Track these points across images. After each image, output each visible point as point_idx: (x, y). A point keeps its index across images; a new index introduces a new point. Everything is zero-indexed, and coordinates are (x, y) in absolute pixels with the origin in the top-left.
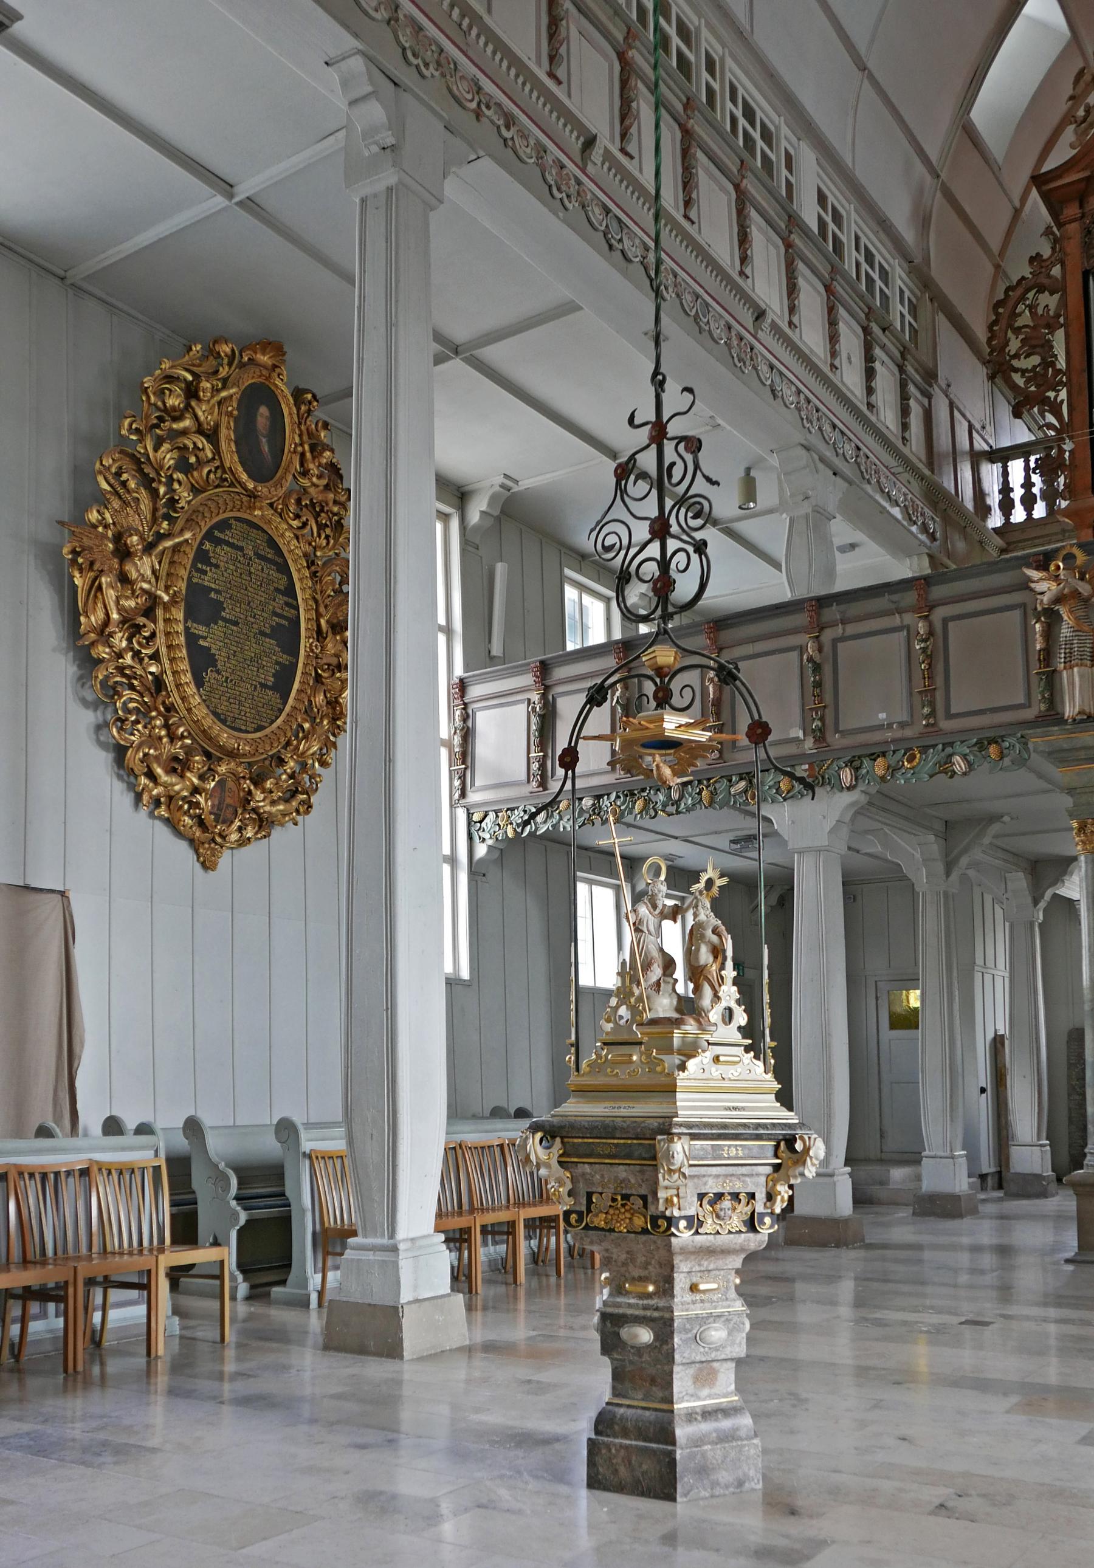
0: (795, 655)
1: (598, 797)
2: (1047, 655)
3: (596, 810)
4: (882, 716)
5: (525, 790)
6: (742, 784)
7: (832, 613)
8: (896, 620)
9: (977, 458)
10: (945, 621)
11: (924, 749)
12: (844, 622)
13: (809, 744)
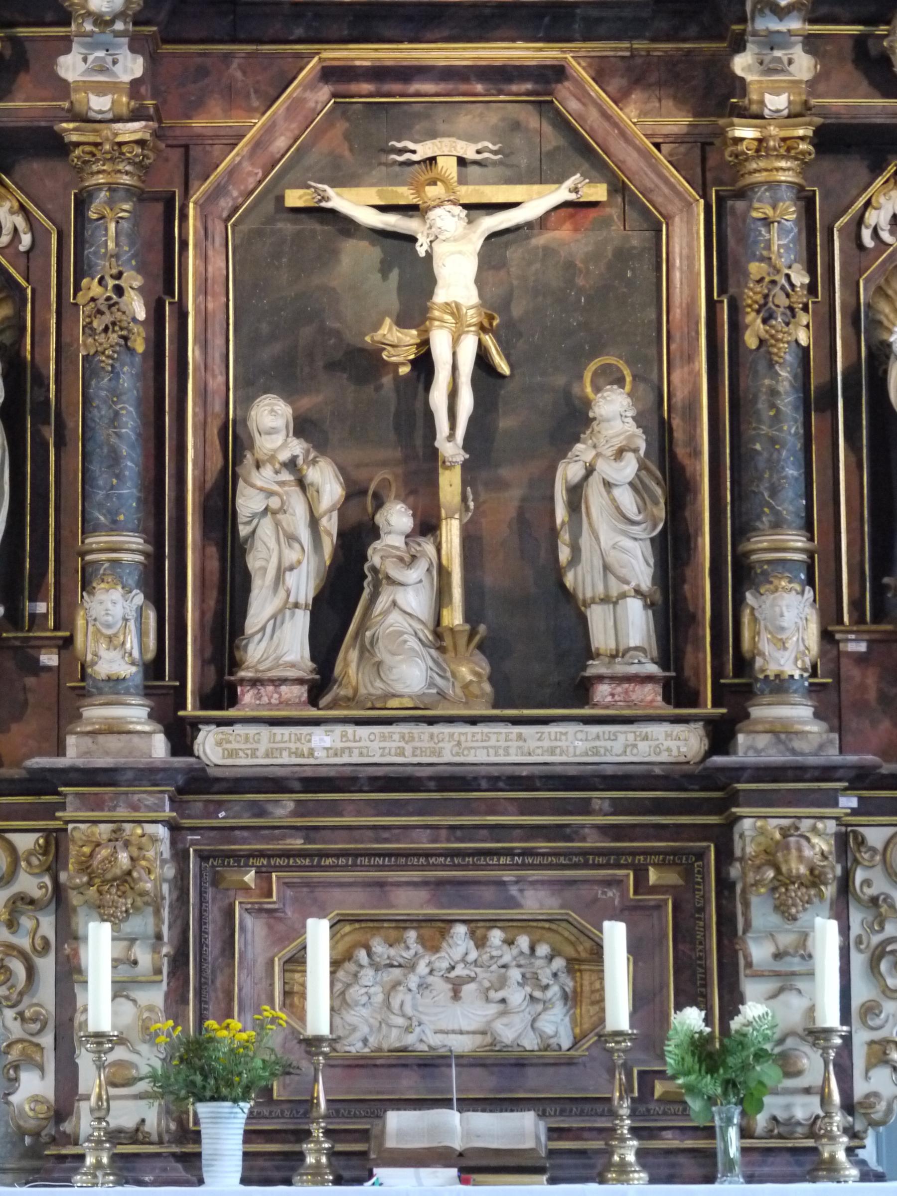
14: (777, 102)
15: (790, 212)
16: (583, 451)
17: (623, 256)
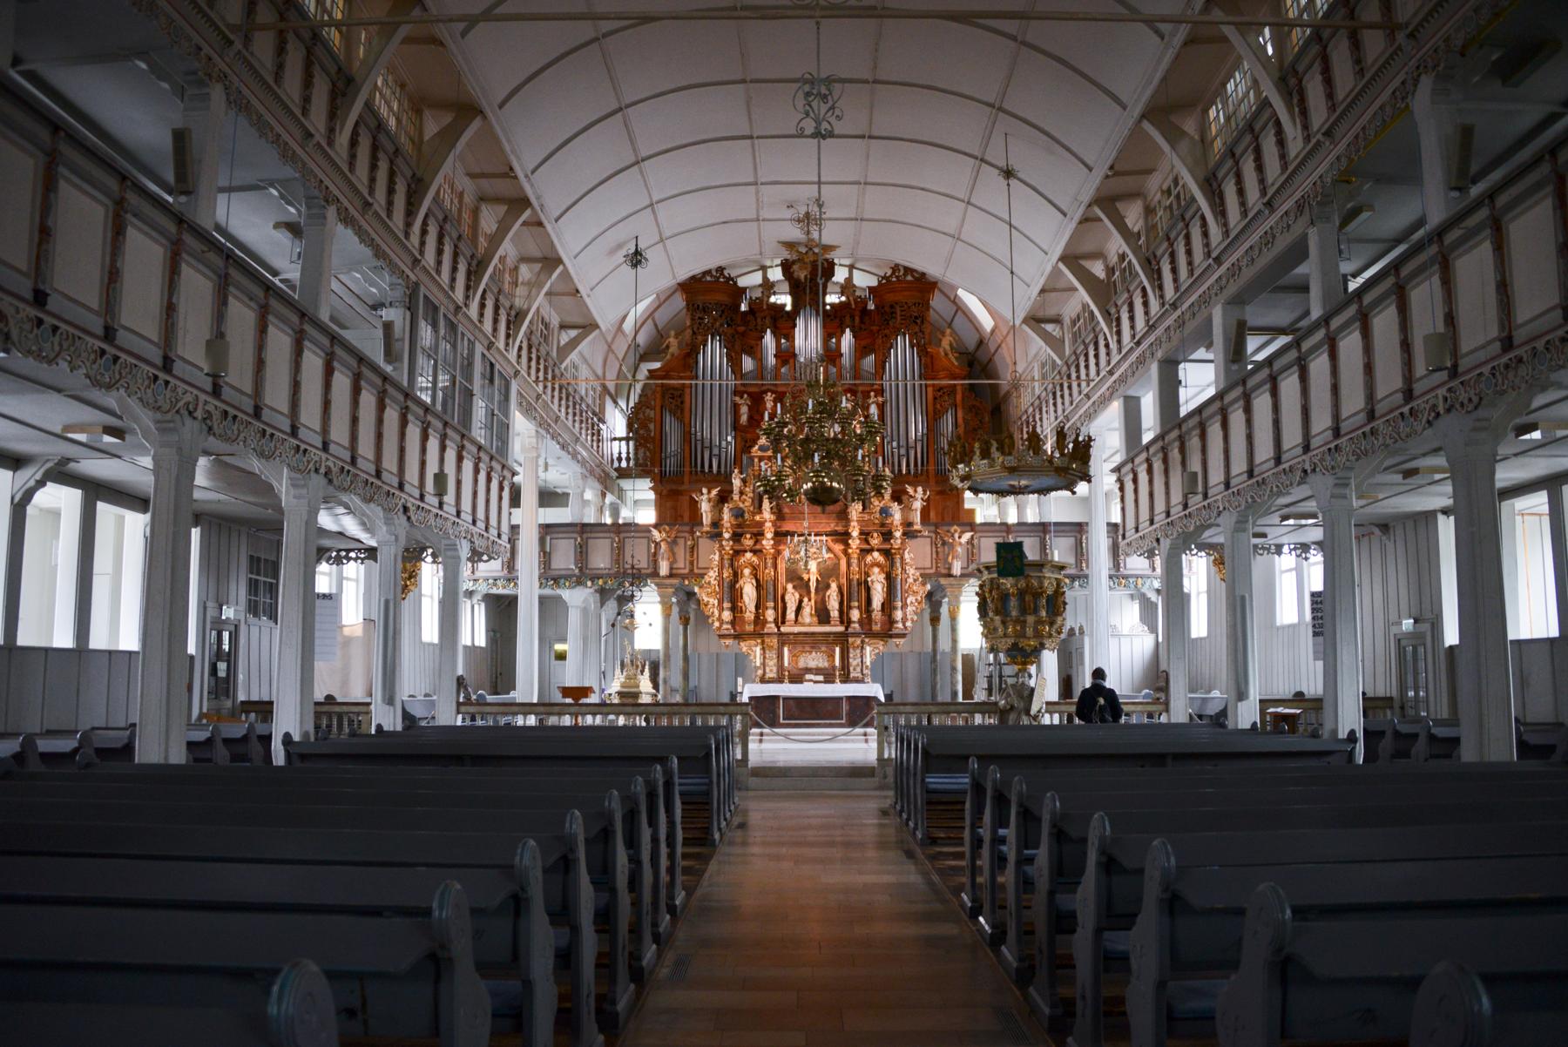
0: (573, 541)
2: (655, 554)
4: (602, 565)
7: (588, 529)
8: (608, 535)
10: (624, 538)
13: (577, 571)
15: (856, 561)
17: (835, 564)
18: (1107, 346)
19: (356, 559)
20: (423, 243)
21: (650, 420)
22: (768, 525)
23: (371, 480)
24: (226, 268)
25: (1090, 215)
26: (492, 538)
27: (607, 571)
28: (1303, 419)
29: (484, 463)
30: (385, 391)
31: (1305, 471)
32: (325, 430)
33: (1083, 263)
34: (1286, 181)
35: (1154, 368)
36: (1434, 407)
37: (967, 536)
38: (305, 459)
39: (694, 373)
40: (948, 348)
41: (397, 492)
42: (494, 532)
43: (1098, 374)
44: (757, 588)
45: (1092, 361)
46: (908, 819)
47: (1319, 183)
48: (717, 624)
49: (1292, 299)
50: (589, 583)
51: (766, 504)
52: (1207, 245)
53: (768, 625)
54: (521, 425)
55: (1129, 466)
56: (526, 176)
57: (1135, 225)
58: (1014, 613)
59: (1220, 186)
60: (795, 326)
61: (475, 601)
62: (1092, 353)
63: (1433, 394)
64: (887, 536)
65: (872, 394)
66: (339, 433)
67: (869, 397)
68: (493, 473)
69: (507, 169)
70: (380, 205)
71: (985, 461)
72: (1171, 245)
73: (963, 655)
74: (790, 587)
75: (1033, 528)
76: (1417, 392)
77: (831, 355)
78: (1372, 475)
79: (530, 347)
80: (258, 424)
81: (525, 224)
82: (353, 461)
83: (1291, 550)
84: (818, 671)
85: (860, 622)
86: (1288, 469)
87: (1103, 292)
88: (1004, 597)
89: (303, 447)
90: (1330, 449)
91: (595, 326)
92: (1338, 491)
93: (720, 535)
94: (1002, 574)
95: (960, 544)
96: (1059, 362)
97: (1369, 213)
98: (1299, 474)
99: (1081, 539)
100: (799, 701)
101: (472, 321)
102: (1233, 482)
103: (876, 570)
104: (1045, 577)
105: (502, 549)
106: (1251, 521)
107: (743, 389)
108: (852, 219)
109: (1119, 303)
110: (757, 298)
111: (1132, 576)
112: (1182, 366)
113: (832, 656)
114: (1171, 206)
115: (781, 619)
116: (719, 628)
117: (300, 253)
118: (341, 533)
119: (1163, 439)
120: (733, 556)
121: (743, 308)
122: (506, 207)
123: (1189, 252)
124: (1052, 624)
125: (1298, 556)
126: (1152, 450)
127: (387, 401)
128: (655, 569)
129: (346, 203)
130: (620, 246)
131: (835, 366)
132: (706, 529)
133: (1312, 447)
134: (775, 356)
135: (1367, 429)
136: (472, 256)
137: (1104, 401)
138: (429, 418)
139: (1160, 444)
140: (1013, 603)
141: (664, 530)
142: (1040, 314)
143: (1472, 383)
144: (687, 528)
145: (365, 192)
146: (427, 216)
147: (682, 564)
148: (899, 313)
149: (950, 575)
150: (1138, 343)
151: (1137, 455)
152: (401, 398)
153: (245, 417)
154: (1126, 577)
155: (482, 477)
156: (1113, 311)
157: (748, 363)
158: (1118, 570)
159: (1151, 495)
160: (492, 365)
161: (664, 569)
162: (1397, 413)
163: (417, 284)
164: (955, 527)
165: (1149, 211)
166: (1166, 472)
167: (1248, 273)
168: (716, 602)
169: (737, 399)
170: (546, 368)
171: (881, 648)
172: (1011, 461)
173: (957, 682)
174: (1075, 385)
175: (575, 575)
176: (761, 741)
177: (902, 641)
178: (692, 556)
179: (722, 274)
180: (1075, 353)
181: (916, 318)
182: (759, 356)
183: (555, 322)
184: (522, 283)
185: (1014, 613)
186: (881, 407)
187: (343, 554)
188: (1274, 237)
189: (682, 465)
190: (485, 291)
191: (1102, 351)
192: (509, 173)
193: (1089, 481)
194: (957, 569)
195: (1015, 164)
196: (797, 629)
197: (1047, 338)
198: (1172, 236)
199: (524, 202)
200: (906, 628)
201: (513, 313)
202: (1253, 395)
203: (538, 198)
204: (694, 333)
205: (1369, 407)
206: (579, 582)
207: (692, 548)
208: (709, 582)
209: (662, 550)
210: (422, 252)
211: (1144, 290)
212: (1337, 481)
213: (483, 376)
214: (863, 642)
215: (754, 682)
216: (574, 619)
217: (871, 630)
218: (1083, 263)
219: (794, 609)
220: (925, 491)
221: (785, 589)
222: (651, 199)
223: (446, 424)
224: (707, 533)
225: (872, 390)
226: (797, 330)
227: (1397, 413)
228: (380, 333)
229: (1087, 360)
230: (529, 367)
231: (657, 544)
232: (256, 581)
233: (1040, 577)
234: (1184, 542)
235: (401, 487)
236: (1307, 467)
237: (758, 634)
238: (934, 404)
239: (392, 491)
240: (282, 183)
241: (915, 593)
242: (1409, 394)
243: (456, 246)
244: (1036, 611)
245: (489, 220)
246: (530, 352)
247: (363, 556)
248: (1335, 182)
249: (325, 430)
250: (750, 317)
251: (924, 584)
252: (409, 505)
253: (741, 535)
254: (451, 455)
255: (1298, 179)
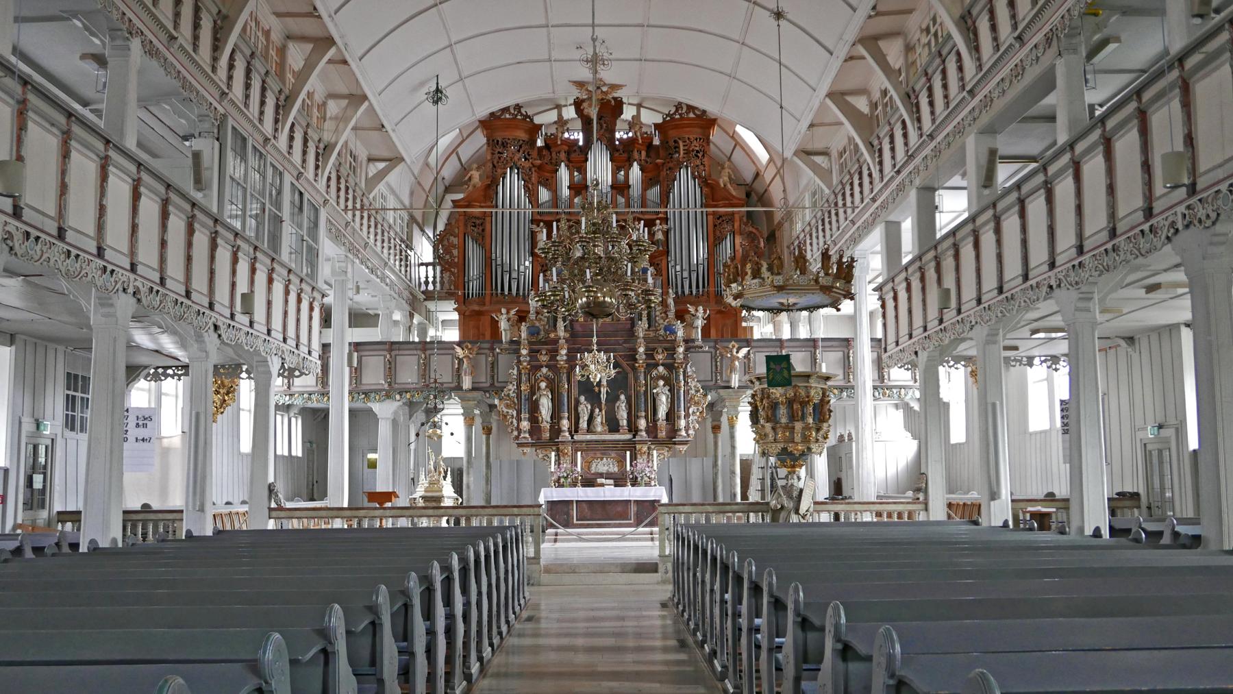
0: (382, 357)
1: (310, 394)
3: (309, 399)
5: (282, 389)
6: (363, 396)
8: (415, 352)
9: (419, 266)
11: (422, 392)
12: (399, 350)
13: (386, 386)
14: (641, 362)
15: (643, 375)
16: (619, 402)
18: (870, 175)
19: (172, 377)
20: (230, 78)
21: (454, 246)
22: (562, 341)
23: (181, 299)
24: (24, 93)
25: (854, 54)
26: (302, 355)
27: (414, 386)
28: (1049, 239)
29: (294, 285)
30: (193, 216)
31: (1051, 287)
32: (133, 252)
33: (849, 99)
34: (1036, 15)
35: (913, 195)
36: (1173, 224)
37: (744, 351)
38: (112, 280)
39: (494, 202)
40: (726, 179)
41: (207, 312)
42: (304, 349)
43: (862, 201)
44: (552, 399)
45: (857, 189)
46: (683, 611)
47: (1067, 14)
48: (515, 433)
49: (1043, 127)
50: (398, 397)
51: (561, 325)
52: (962, 79)
53: (562, 434)
54: (328, 248)
55: (890, 285)
56: (330, 16)
57: (895, 63)
58: (784, 420)
59: (974, 23)
60: (587, 160)
61: (292, 414)
62: (856, 182)
63: (1173, 212)
64: (671, 350)
65: (658, 222)
66: (148, 254)
67: (655, 225)
68: (303, 295)
69: (311, 9)
70: (186, 40)
71: (756, 281)
72: (929, 80)
73: (742, 461)
74: (582, 398)
75: (806, 343)
76: (1156, 211)
77: (620, 188)
78: (1114, 290)
79: (339, 178)
80: (62, 245)
81: (330, 61)
82: (162, 282)
83: (1042, 362)
84: (608, 476)
85: (647, 431)
86: (1035, 285)
87: (866, 125)
88: (774, 406)
89: (110, 267)
90: (1074, 266)
91: (402, 159)
92: (1081, 305)
93: (517, 352)
94: (772, 384)
95: (738, 358)
96: (827, 191)
97: (1116, 45)
98: (1045, 289)
99: (848, 353)
100: (590, 503)
101: (281, 153)
102: (984, 298)
103: (661, 383)
104: (811, 387)
105: (313, 365)
106: (1001, 334)
107: (539, 217)
108: (637, 60)
109: (881, 136)
110: (552, 135)
111: (895, 387)
112: (937, 193)
113: (622, 462)
114: (929, 43)
115: (575, 429)
116: (517, 438)
117: (105, 83)
118: (157, 351)
119: (921, 260)
120: (529, 371)
121: (540, 143)
122: (311, 46)
123: (945, 87)
124: (818, 430)
125: (1049, 367)
126: (910, 270)
127: (196, 226)
128: (459, 383)
129: (150, 36)
130: (422, 84)
131: (623, 196)
132: (505, 346)
133: (1057, 264)
134: (569, 187)
135: (1109, 246)
136: (280, 92)
137: (867, 227)
138: (239, 242)
139: (918, 264)
140: (782, 411)
141: (467, 347)
142: (809, 147)
143: (1210, 200)
144: (487, 345)
145: (170, 26)
146: (233, 51)
147: (484, 379)
148: (682, 148)
149: (729, 387)
150: (898, 172)
151: (896, 276)
152: (211, 223)
153: (48, 238)
154: (890, 388)
155: (292, 298)
156: (876, 142)
157: (544, 194)
158: (883, 381)
159: (910, 312)
160: (301, 194)
161: (467, 383)
162: (1137, 230)
163: (224, 115)
164: (733, 343)
165: (909, 48)
166: (923, 289)
167: (999, 104)
168: (515, 413)
169: (534, 226)
170: (354, 198)
171: (666, 454)
172: (779, 280)
173: (735, 485)
174: (841, 211)
175: (384, 390)
176: (555, 541)
177: (685, 447)
178: (492, 370)
179: (519, 111)
180: (841, 182)
181: (698, 152)
182: (554, 188)
183: (362, 154)
184: (331, 118)
185: (784, 420)
186: (666, 233)
187: (160, 371)
188: (1024, 69)
189: (483, 287)
190: (293, 125)
191: (866, 180)
192: (313, 13)
193: (852, 299)
194: (735, 381)
195: (785, 7)
196: (589, 437)
197: (815, 168)
198: (930, 71)
199: (329, 41)
200: (688, 435)
201: (322, 146)
202: (1003, 218)
203: (342, 37)
204: (494, 166)
205: (1111, 225)
206: (388, 396)
207: (493, 364)
208: (508, 395)
209: (465, 366)
210: (229, 86)
211: (904, 122)
212: (1081, 296)
213: (292, 203)
214: (649, 448)
215: (549, 486)
216: (384, 430)
217: (656, 437)
218: (849, 99)
219: (586, 418)
220: (705, 311)
221: (578, 403)
222: (450, 40)
223: (256, 248)
224: (506, 350)
225: (658, 219)
226: (588, 163)
227: (1137, 230)
228: (190, 161)
229: (852, 189)
230: (338, 197)
231: (461, 361)
232: (74, 397)
233: (806, 387)
234: (941, 354)
235: (211, 306)
236: (1053, 283)
237: (553, 441)
238: (714, 231)
239: (202, 310)
240: (87, 15)
241: (697, 404)
242: (1149, 213)
243: (264, 82)
244: (803, 418)
245: (296, 56)
246: (338, 182)
247: (180, 372)
248: (1083, 15)
249: (133, 252)
250: (544, 152)
251: (705, 395)
252: (219, 323)
253: (538, 351)
254: (261, 277)
255: (1047, 13)
